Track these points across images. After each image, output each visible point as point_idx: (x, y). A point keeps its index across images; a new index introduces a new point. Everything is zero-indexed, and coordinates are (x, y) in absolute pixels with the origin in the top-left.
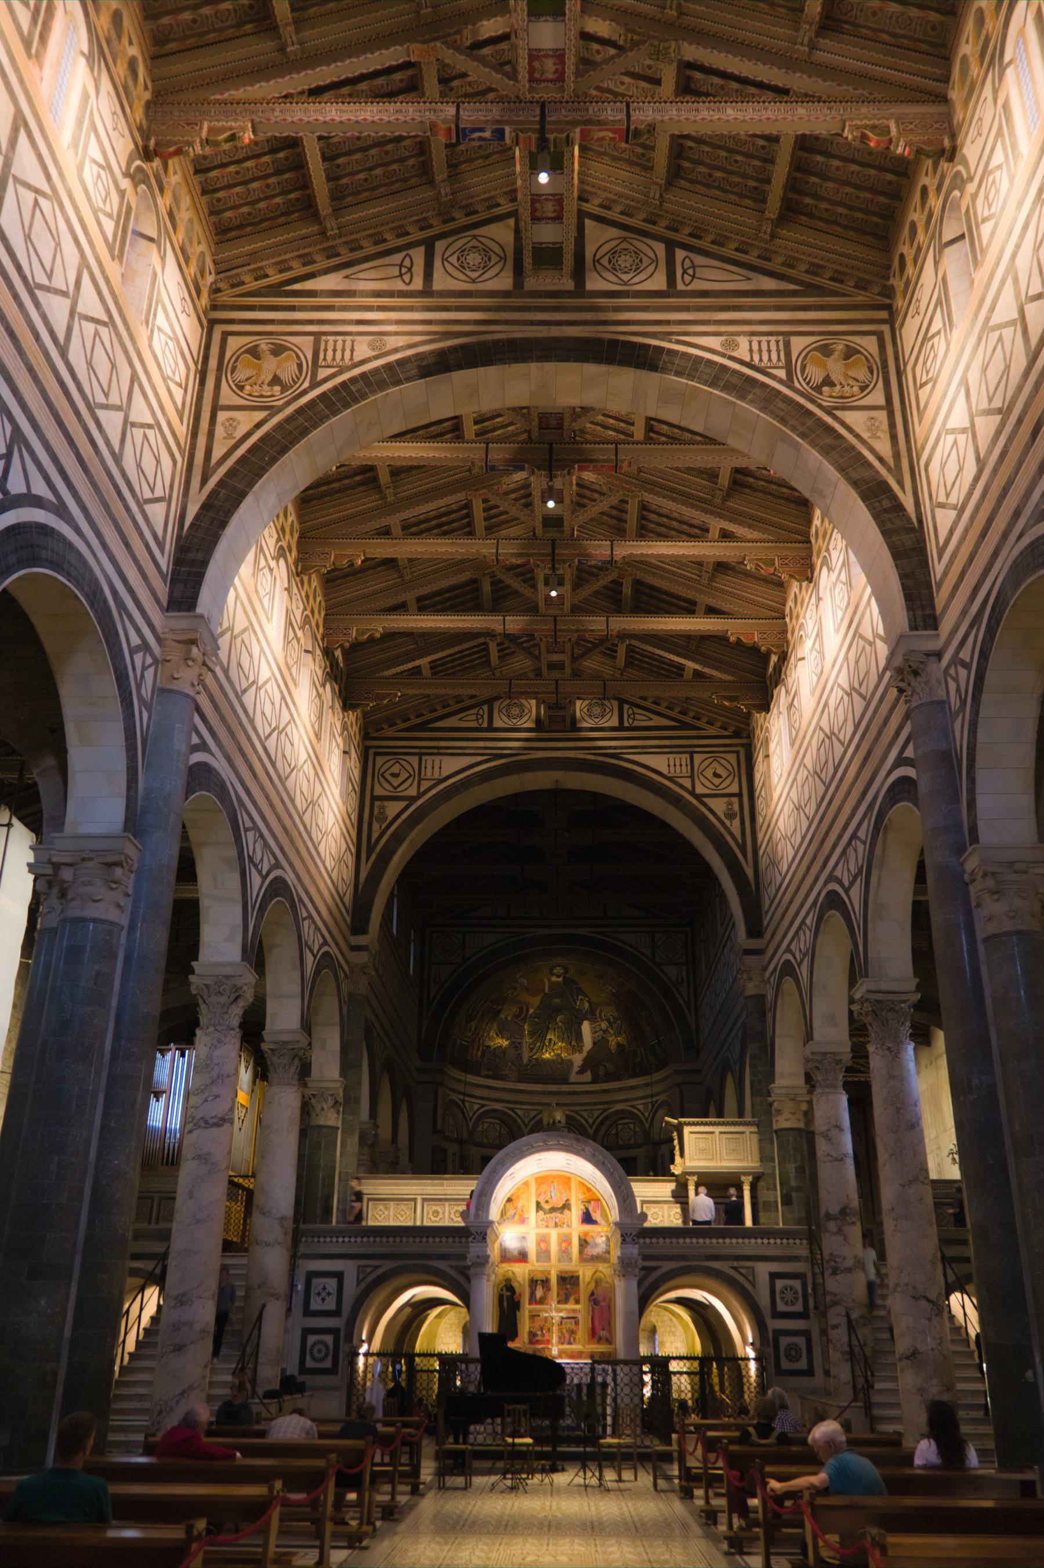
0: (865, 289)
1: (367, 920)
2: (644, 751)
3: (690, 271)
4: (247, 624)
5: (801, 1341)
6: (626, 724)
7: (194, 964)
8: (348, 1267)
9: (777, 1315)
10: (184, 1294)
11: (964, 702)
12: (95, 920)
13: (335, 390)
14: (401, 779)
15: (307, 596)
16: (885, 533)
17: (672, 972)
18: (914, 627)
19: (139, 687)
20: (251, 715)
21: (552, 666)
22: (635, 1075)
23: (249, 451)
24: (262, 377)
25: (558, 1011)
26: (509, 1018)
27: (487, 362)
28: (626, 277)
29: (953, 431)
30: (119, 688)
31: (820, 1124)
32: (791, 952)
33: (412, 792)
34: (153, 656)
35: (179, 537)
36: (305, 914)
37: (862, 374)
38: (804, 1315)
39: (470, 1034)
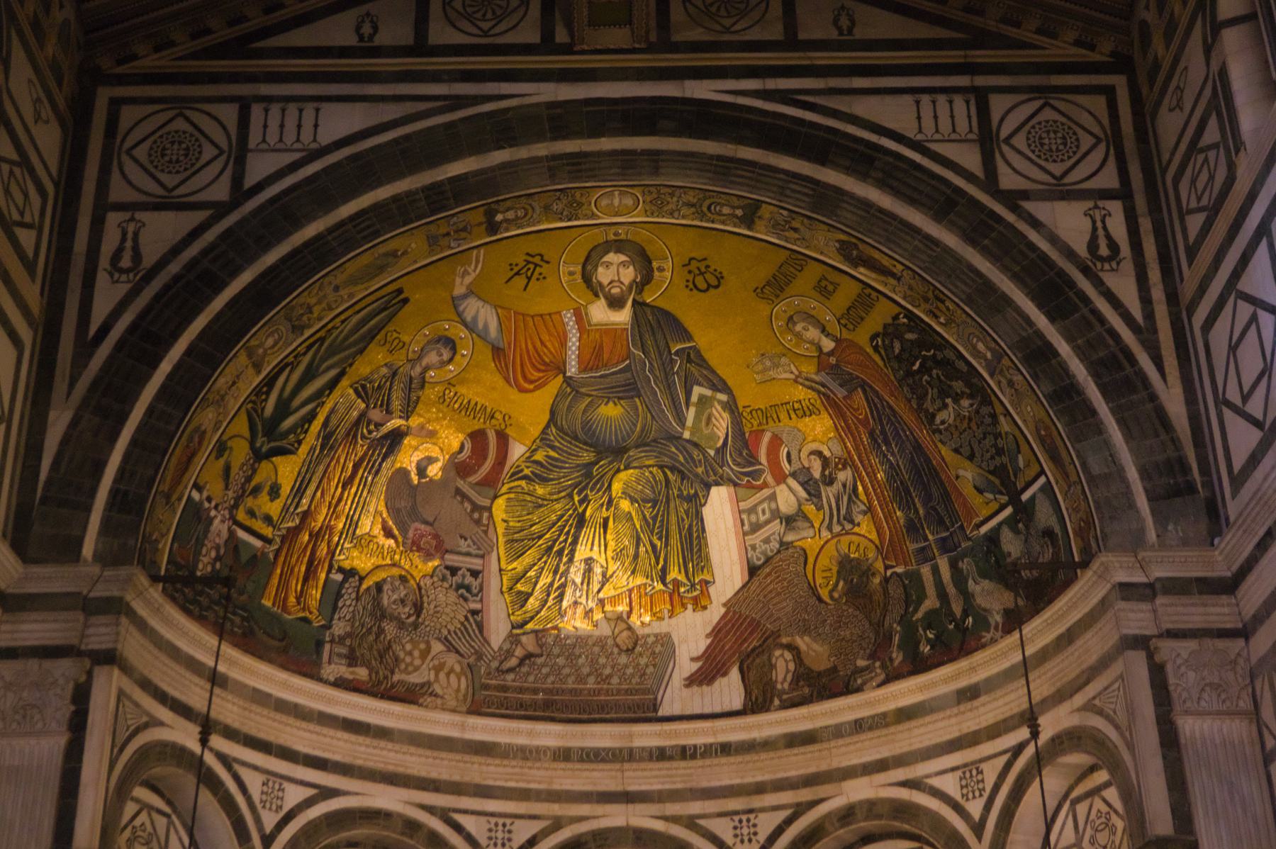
22: (918, 665)
26: (434, 471)
39: (274, 508)
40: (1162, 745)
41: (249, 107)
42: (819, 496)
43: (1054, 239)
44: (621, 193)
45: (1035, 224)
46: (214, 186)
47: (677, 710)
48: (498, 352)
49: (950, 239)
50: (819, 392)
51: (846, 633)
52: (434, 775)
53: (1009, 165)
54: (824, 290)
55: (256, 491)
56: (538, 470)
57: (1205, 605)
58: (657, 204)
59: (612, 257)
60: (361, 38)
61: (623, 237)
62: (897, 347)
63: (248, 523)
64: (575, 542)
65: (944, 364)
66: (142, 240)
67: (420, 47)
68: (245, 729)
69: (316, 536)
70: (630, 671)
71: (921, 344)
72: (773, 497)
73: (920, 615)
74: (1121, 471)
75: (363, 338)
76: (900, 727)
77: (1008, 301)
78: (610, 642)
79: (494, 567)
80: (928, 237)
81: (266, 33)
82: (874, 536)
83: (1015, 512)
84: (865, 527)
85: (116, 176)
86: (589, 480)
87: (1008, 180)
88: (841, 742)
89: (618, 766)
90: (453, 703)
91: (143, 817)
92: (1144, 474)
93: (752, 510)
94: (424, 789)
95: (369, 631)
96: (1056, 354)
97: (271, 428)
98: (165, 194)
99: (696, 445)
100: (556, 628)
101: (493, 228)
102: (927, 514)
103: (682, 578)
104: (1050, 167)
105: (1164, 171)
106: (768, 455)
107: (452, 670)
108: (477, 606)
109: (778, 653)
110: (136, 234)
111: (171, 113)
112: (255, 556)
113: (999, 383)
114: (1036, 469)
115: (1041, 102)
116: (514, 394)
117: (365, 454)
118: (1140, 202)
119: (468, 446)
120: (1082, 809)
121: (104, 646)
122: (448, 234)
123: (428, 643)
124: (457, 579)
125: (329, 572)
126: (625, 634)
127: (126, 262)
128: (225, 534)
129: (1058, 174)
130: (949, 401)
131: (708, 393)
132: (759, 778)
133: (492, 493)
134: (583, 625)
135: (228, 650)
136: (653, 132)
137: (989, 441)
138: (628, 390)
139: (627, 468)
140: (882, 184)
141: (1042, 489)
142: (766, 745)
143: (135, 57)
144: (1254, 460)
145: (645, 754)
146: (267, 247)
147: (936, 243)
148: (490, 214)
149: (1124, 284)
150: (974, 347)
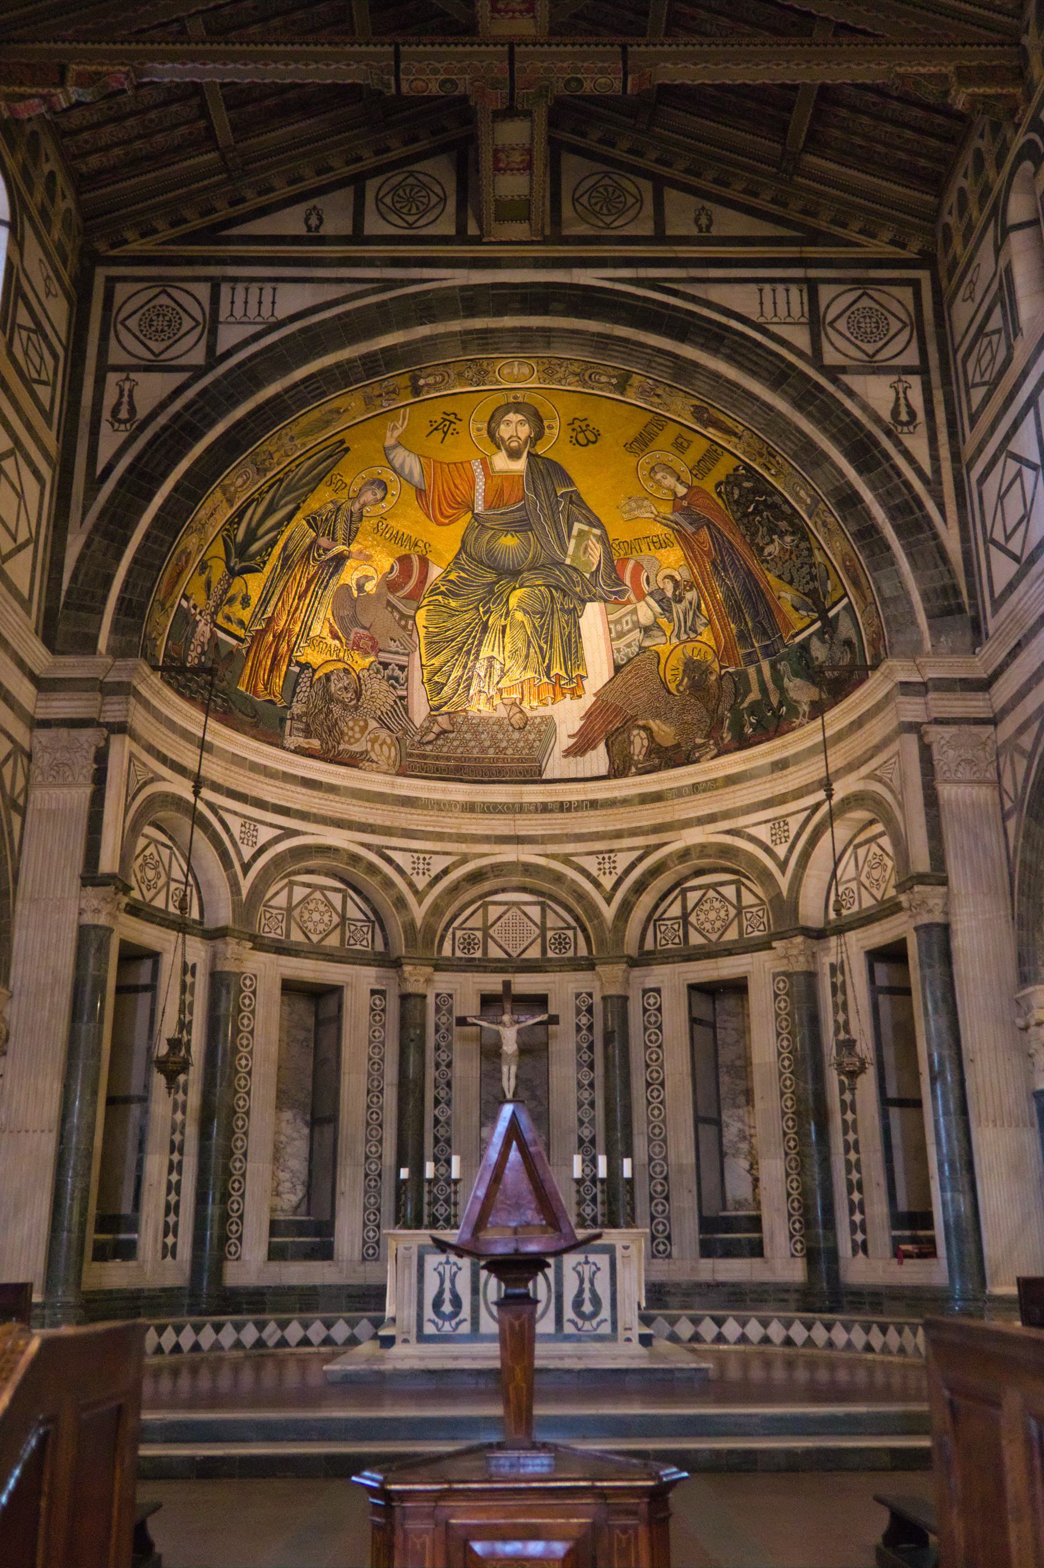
22: (743, 743)
25: (512, 574)
26: (370, 587)
39: (246, 615)
40: (926, 805)
41: (219, 285)
42: (671, 612)
43: (865, 407)
44: (521, 364)
45: (850, 393)
46: (192, 352)
47: (557, 776)
48: (420, 493)
49: (782, 405)
50: (673, 529)
51: (688, 718)
52: (371, 821)
53: (832, 344)
54: (680, 446)
55: (231, 601)
56: (452, 587)
57: (964, 700)
58: (549, 373)
59: (512, 417)
60: (309, 229)
61: (520, 400)
62: (736, 492)
63: (225, 626)
64: (480, 644)
65: (773, 507)
66: (136, 398)
67: (357, 237)
68: (227, 784)
69: (278, 637)
70: (521, 744)
71: (755, 491)
72: (634, 611)
73: (745, 705)
74: (907, 594)
75: (314, 479)
76: (727, 790)
77: (826, 457)
78: (506, 722)
79: (417, 663)
80: (765, 404)
82: (712, 643)
83: (823, 626)
84: (706, 636)
85: (113, 343)
86: (492, 596)
87: (831, 357)
88: (681, 800)
89: (510, 816)
90: (385, 767)
91: (152, 849)
92: (925, 597)
93: (618, 621)
94: (364, 831)
95: (321, 711)
96: (861, 500)
97: (242, 551)
98: (151, 357)
99: (575, 569)
100: (465, 710)
101: (416, 391)
102: (755, 626)
103: (563, 673)
104: (864, 346)
105: (956, 352)
106: (632, 577)
107: (384, 742)
108: (404, 693)
109: (635, 732)
110: (131, 391)
111: (157, 290)
112: (231, 652)
113: (815, 523)
114: (842, 592)
115: (860, 292)
116: (433, 527)
117: (316, 573)
118: (935, 378)
119: (397, 567)
120: (862, 852)
121: (118, 720)
122: (380, 395)
123: (365, 721)
124: (388, 672)
125: (289, 665)
126: (518, 716)
127: (124, 414)
128: (208, 635)
129: (871, 353)
130: (775, 537)
131: (586, 528)
132: (618, 827)
133: (415, 605)
134: (485, 709)
135: (212, 724)
136: (546, 312)
137: (805, 569)
138: (522, 525)
139: (521, 587)
140: (730, 359)
141: (845, 608)
142: (625, 802)
143: (126, 242)
144: (1011, 587)
145: (532, 808)
146: (235, 404)
147: (771, 408)
148: (415, 379)
149: (918, 444)
150: (797, 494)
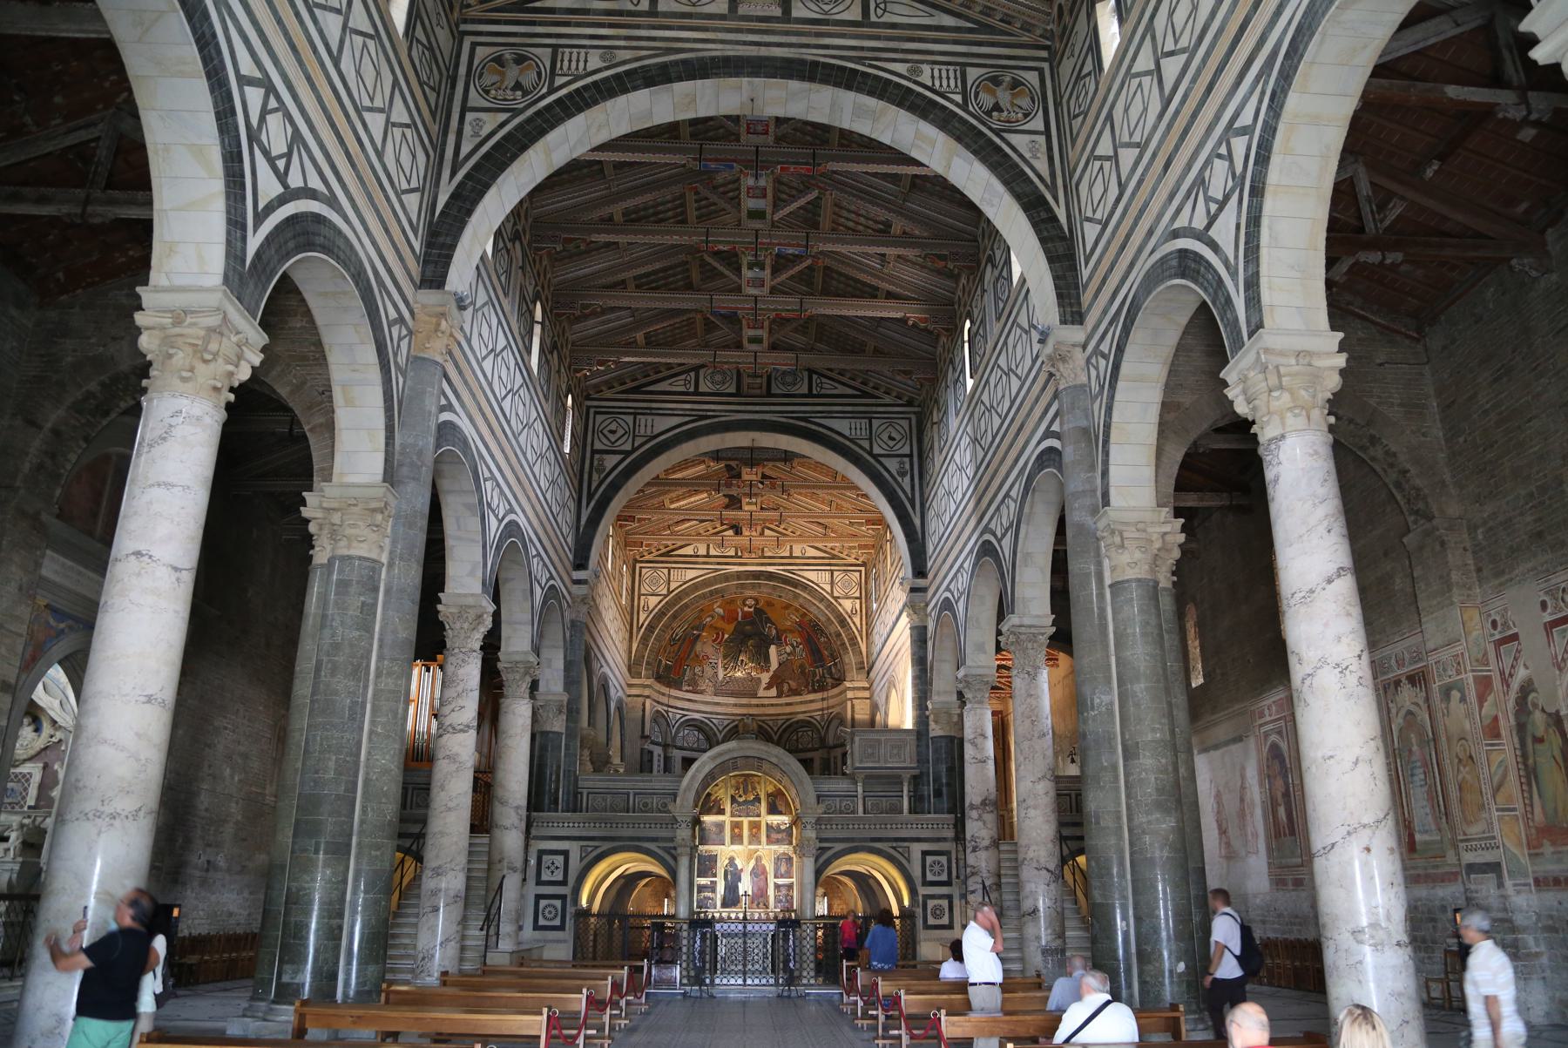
0: (1029, 31)
1: (587, 558)
2: (830, 415)
3: (882, 6)
4: (486, 298)
5: (945, 903)
6: (815, 392)
7: (440, 595)
8: (574, 848)
9: (926, 883)
10: (439, 867)
11: (1102, 387)
12: (360, 558)
13: (570, 95)
14: (618, 435)
15: (539, 274)
16: (1043, 241)
17: (847, 605)
18: (1063, 322)
19: (395, 355)
20: (490, 378)
21: (753, 340)
22: (815, 691)
23: (493, 148)
24: (506, 83)
25: (749, 637)
27: (704, 75)
28: (827, 8)
29: (1099, 158)
30: (379, 356)
31: (968, 733)
32: (950, 591)
33: (628, 447)
34: (408, 328)
35: (431, 223)
36: (534, 553)
37: (1025, 102)
38: (948, 883)
67: (708, 556)
81: (673, 550)
86: (743, 642)
138: (752, 623)
